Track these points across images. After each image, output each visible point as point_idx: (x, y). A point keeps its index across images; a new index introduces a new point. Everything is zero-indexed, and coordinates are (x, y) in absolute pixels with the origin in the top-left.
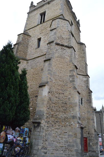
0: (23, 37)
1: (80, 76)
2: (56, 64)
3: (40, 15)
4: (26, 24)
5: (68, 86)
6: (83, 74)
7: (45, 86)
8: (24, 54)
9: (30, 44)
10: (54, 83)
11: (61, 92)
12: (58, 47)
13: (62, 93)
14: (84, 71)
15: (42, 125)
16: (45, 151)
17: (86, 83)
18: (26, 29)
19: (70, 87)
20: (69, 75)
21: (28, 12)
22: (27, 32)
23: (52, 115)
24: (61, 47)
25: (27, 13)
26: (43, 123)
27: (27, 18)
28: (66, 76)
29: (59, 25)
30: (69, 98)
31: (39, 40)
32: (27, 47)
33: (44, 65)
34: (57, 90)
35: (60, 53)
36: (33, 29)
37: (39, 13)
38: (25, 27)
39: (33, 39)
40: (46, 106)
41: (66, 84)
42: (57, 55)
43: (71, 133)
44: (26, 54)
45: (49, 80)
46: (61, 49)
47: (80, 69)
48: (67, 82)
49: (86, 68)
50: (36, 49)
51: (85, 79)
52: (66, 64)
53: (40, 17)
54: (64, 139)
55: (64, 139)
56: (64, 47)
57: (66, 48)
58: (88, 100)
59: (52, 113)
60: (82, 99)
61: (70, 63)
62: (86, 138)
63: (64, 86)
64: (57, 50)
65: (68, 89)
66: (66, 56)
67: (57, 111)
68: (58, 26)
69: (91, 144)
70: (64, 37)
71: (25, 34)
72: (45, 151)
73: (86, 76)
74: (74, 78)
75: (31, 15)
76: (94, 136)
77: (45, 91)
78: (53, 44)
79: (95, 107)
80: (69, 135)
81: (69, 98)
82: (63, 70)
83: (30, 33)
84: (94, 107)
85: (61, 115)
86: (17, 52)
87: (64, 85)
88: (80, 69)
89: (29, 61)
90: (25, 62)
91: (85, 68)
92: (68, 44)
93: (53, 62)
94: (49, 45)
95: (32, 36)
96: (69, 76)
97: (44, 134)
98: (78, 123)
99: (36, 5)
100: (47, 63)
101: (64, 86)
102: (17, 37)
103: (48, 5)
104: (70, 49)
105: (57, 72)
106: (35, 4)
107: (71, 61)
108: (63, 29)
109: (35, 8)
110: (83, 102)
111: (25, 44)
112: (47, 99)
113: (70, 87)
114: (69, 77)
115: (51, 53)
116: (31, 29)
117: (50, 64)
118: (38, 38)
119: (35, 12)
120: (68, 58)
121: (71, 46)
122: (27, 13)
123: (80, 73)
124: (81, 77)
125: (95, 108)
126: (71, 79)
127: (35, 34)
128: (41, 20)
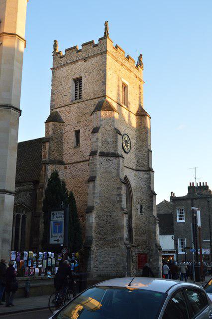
0: (53, 126)
1: (139, 172)
4: (53, 94)
6: (143, 169)
7: (91, 212)
8: (58, 154)
9: (65, 137)
11: (108, 214)
12: (103, 159)
14: (145, 163)
15: (93, 249)
16: (96, 269)
17: (148, 183)
18: (53, 104)
21: (52, 67)
22: (57, 112)
23: (101, 238)
24: (106, 158)
26: (94, 248)
27: (52, 80)
29: (102, 123)
30: (117, 220)
31: (77, 132)
32: (62, 142)
33: (88, 186)
35: (105, 167)
36: (66, 108)
38: (52, 101)
39: (67, 129)
40: (93, 232)
42: (102, 170)
43: (118, 253)
44: (61, 154)
45: (95, 205)
47: (140, 161)
49: (148, 158)
50: (75, 147)
51: (146, 176)
53: (74, 85)
54: (113, 259)
55: (113, 259)
56: (109, 158)
58: (149, 207)
59: (101, 237)
60: (141, 206)
62: (146, 254)
67: (105, 234)
68: (101, 125)
69: (151, 260)
70: (109, 140)
71: (54, 118)
72: (96, 269)
73: (148, 171)
74: (121, 198)
75: (58, 72)
76: (154, 251)
77: (93, 218)
78: (97, 157)
79: (206, 183)
80: (117, 255)
81: (117, 220)
83: (63, 114)
84: (203, 183)
85: (110, 238)
86: (50, 154)
88: (140, 161)
89: (67, 166)
90: (62, 167)
91: (147, 159)
93: (98, 181)
94: (91, 157)
95: (66, 123)
97: (94, 256)
98: (125, 244)
100: (91, 184)
102: (44, 125)
106: (61, 49)
107: (118, 175)
108: (108, 128)
110: (143, 210)
111: (58, 137)
112: (94, 225)
115: (94, 169)
116: (63, 108)
117: (94, 186)
118: (75, 129)
119: (63, 72)
120: (115, 171)
121: (118, 154)
123: (140, 168)
124: (141, 173)
125: (205, 185)
126: (118, 199)
127: (69, 115)
128: (76, 90)
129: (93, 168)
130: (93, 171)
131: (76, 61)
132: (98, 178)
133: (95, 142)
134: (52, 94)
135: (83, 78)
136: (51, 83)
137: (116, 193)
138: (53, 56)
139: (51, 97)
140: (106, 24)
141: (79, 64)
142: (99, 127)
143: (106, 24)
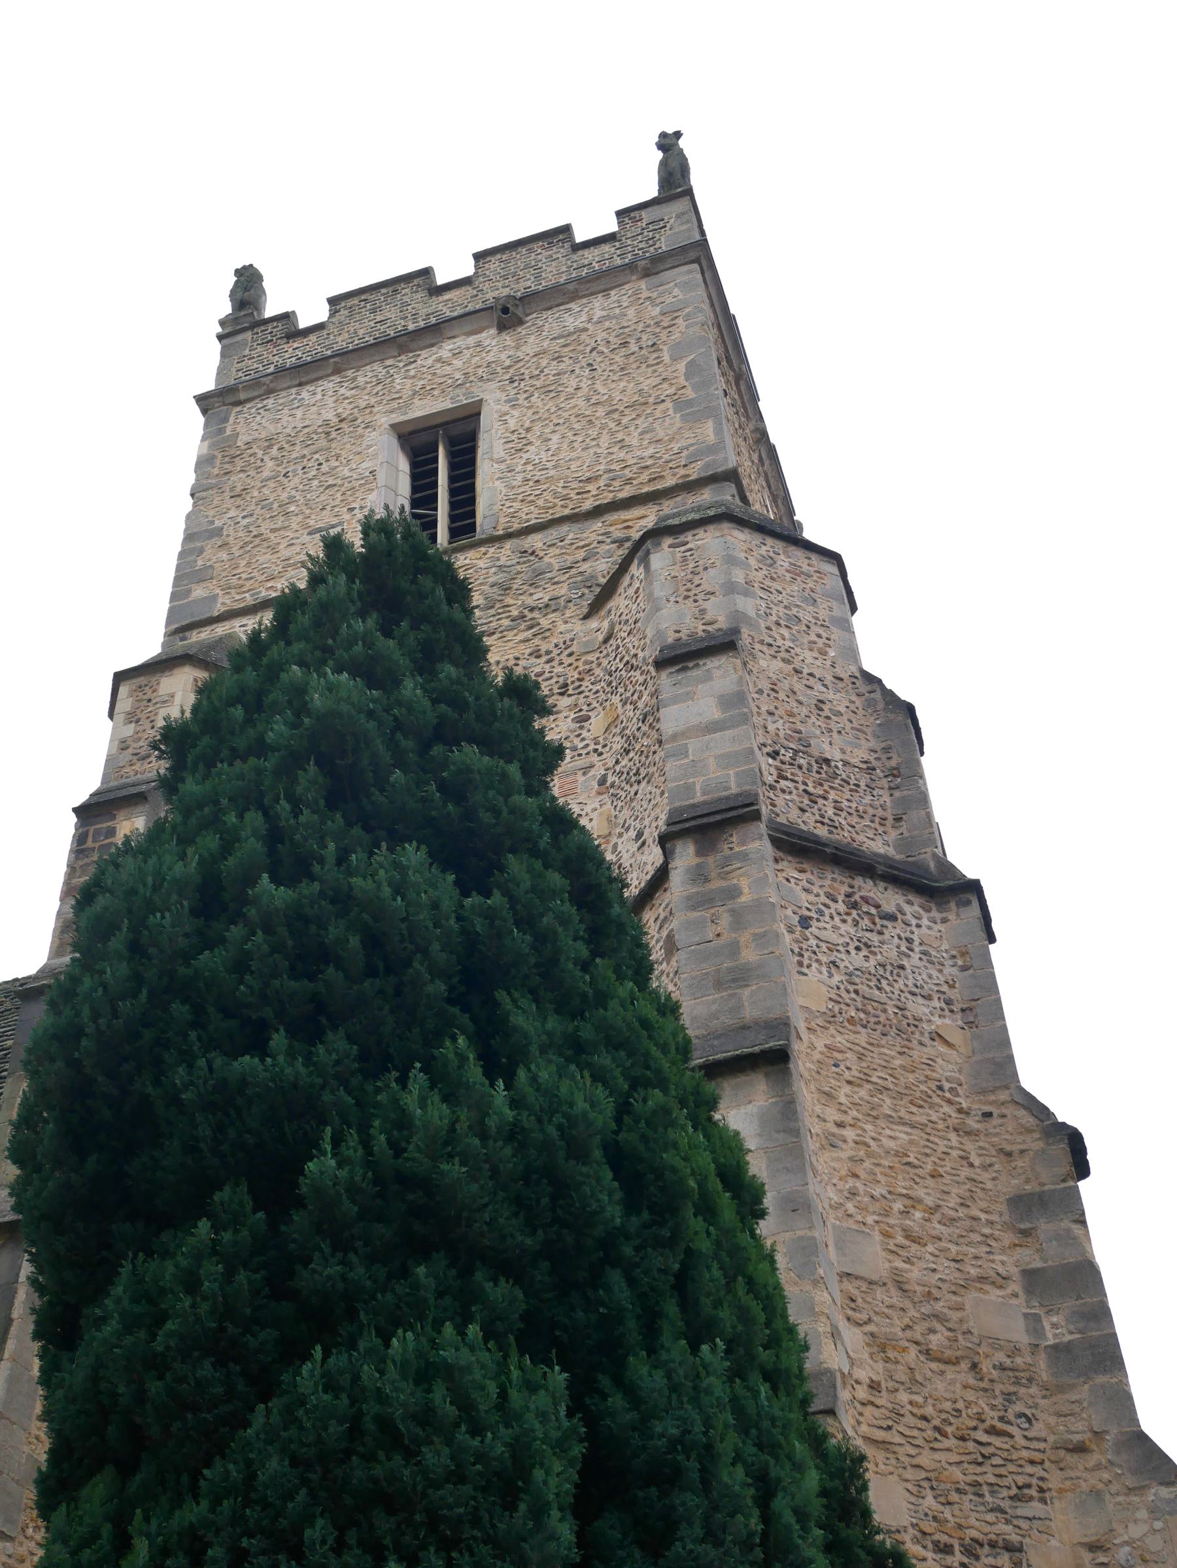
2: (832, 1114)
3: (395, 442)
5: (1038, 1430)
10: (874, 1386)
11: (979, 1524)
13: (993, 1545)
18: (199, 592)
19: (1080, 1449)
20: (1014, 1271)
21: (209, 385)
25: (204, 401)
27: (203, 464)
28: (982, 1279)
34: (929, 1501)
37: (385, 421)
41: (1009, 1397)
46: (841, 907)
48: (1020, 1377)
52: (947, 1109)
53: (404, 465)
56: (867, 888)
57: (891, 899)
61: (983, 1092)
63: (992, 1431)
64: (805, 922)
65: (1055, 1480)
66: (917, 1007)
68: (738, 617)
70: (834, 754)
82: (930, 1201)
87: (992, 1418)
92: (904, 844)
96: (1015, 1287)
99: (312, 313)
101: (992, 1431)
103: (489, 337)
104: (942, 906)
105: (877, 1237)
109: (292, 352)
113: (1080, 1449)
114: (1030, 1290)
115: (749, 955)
122: (204, 401)
129: (734, 949)
130: (740, 977)
131: (434, 331)
132: (802, 1063)
133: (713, 727)
134: (189, 537)
135: (487, 419)
136: (189, 478)
137: (1008, 1262)
138: (220, 337)
139: (182, 555)
140: (668, 143)
141: (446, 349)
142: (736, 631)
143: (668, 143)
